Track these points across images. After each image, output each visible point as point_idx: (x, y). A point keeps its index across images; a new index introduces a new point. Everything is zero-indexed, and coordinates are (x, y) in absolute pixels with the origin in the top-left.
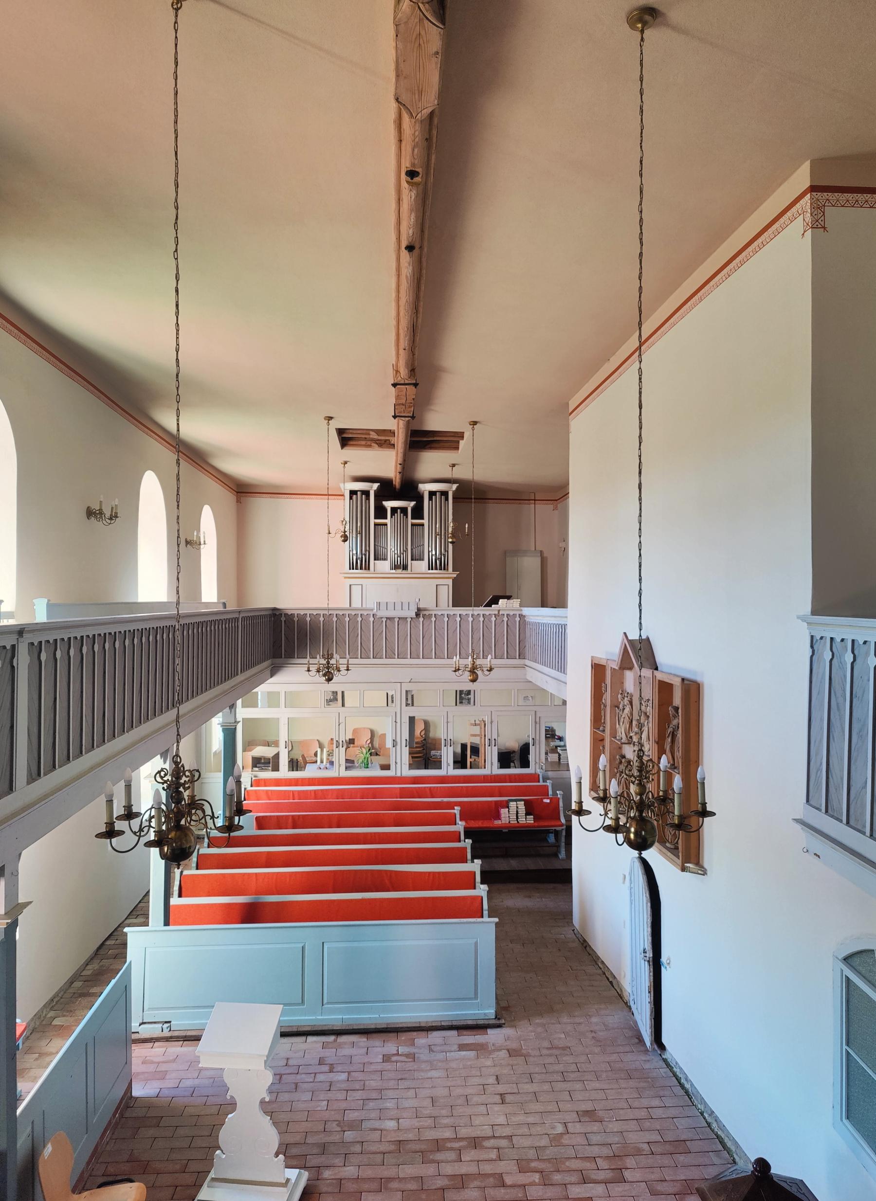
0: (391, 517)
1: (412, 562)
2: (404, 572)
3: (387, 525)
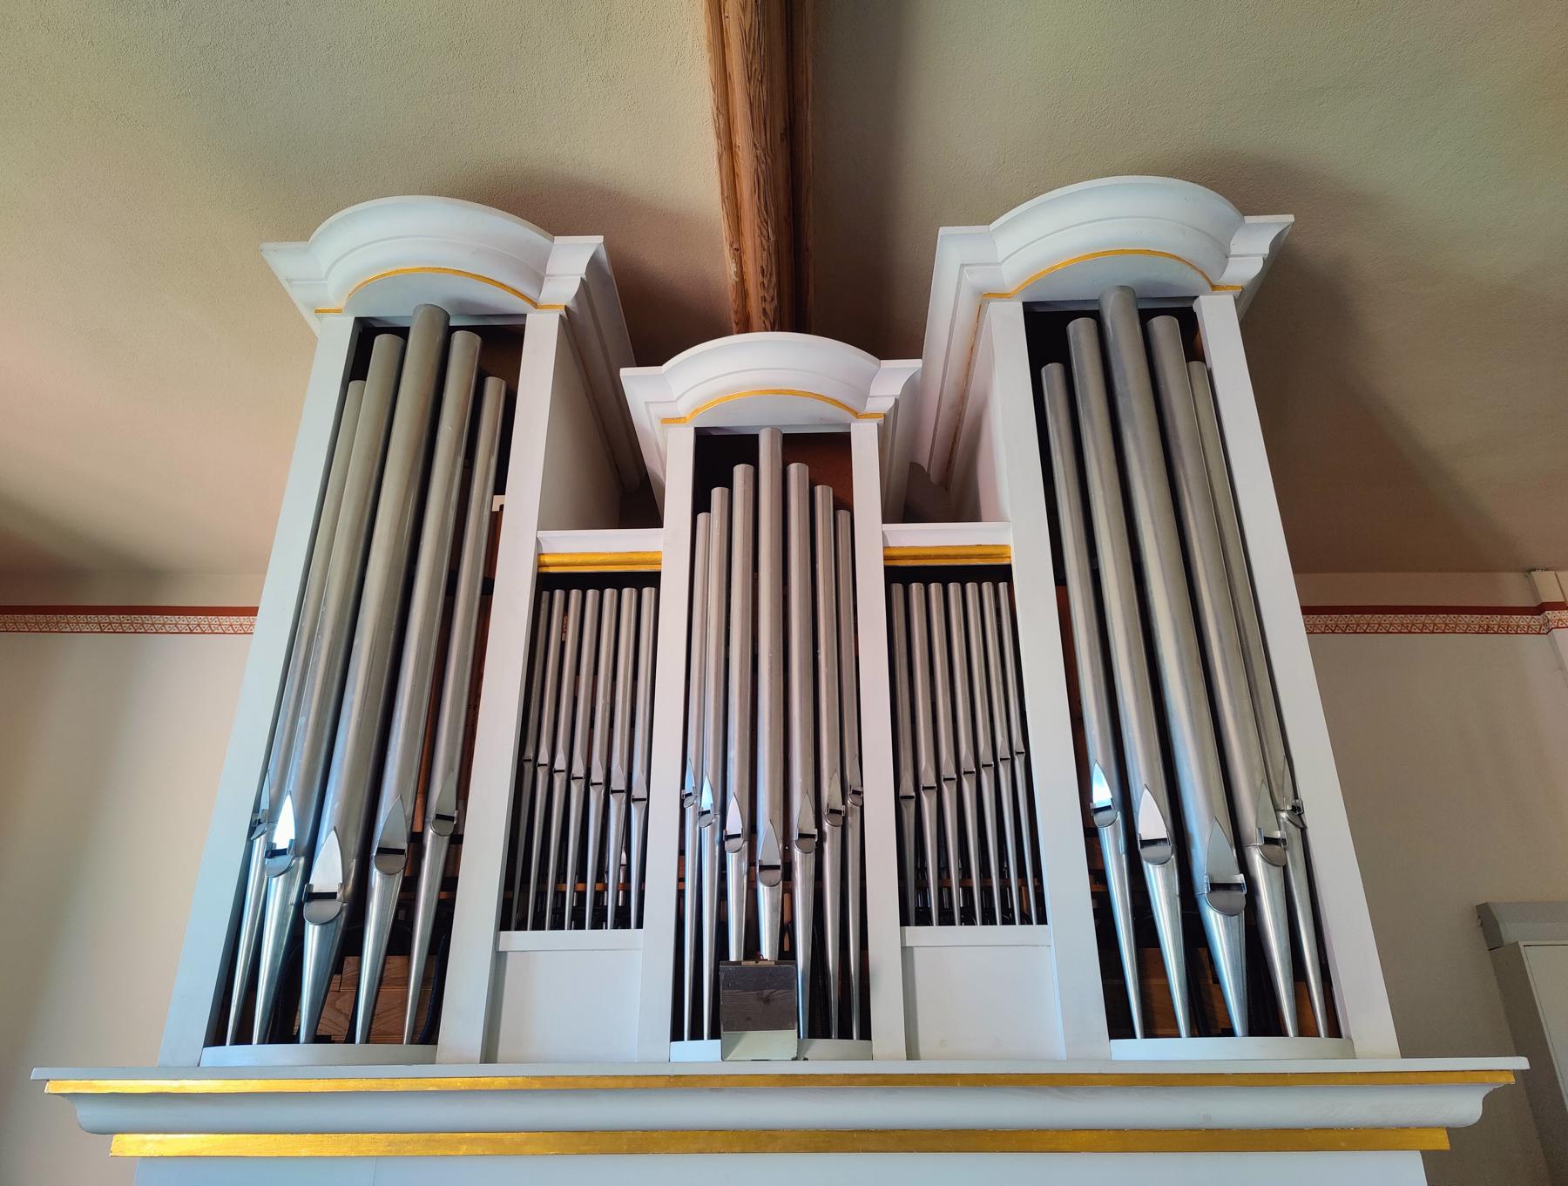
0: (701, 503)
1: (916, 934)
2: (828, 1056)
3: (653, 579)
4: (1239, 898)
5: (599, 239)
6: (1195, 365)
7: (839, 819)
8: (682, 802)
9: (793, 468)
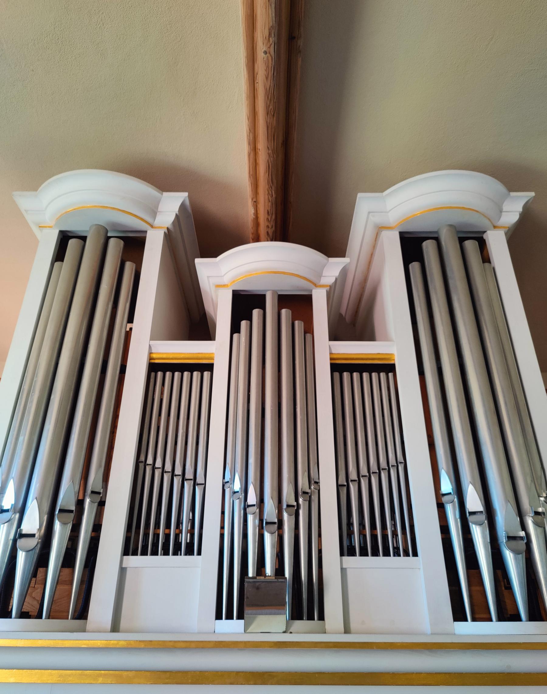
0: (235, 329)
1: (349, 561)
3: (209, 367)
4: (522, 545)
5: (186, 194)
6: (487, 264)
7: (307, 497)
8: (223, 486)
9: (284, 311)
